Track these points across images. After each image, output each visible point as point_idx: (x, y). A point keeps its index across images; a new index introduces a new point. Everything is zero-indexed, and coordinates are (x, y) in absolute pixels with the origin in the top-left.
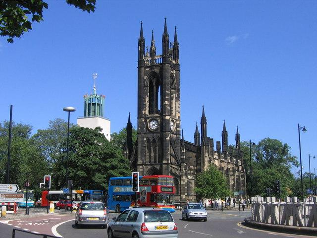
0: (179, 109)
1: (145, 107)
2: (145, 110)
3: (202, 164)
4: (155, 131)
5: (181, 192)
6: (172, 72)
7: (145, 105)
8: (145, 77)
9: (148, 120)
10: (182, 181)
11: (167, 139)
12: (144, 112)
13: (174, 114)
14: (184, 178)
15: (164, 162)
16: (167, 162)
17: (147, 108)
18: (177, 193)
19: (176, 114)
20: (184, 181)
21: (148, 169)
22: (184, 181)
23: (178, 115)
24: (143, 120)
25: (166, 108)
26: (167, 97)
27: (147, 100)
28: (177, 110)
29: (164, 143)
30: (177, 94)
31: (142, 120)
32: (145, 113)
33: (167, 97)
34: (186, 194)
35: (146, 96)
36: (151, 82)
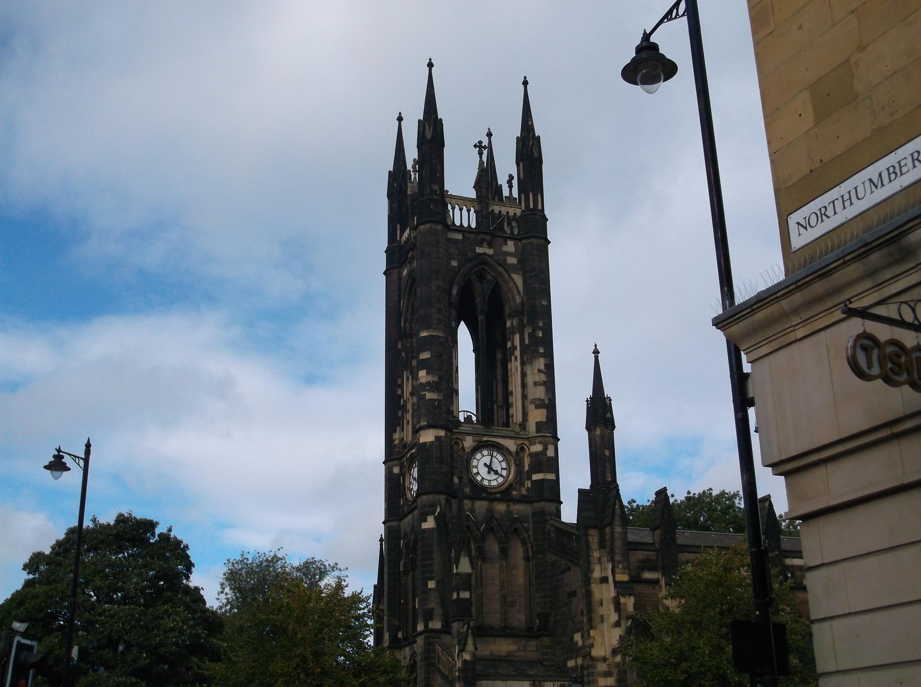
0: (540, 393)
1: (402, 418)
2: (402, 430)
6: (479, 250)
7: (404, 406)
11: (425, 526)
12: (396, 436)
13: (518, 417)
19: (525, 415)
23: (537, 415)
24: (396, 470)
28: (530, 397)
30: (528, 331)
33: (425, 355)
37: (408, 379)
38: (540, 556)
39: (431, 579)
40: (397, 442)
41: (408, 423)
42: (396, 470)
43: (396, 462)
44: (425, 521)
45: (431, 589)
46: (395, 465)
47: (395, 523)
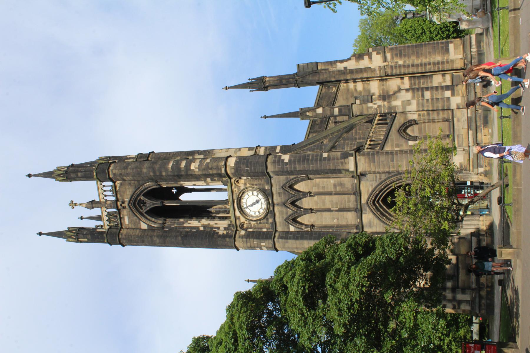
1: (212, 228)
2: (218, 228)
3: (365, 75)
4: (268, 195)
5: (443, 110)
7: (205, 227)
8: (144, 226)
9: (242, 219)
10: (408, 109)
12: (221, 232)
14: (397, 103)
15: (352, 168)
16: (352, 159)
17: (212, 223)
18: (444, 120)
20: (409, 103)
21: (376, 221)
22: (409, 103)
24: (243, 233)
25: (207, 167)
26: (183, 164)
27: (194, 223)
29: (298, 167)
31: (242, 237)
32: (225, 228)
34: (448, 94)
35: (186, 225)
36: (155, 213)
37: (190, 223)
38: (323, 147)
39: (321, 155)
40: (225, 232)
41: (216, 224)
42: (243, 233)
43: (238, 232)
44: (283, 160)
45: (328, 155)
46: (239, 233)
47: (277, 234)
